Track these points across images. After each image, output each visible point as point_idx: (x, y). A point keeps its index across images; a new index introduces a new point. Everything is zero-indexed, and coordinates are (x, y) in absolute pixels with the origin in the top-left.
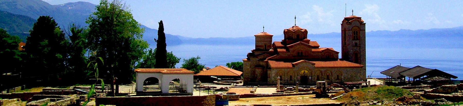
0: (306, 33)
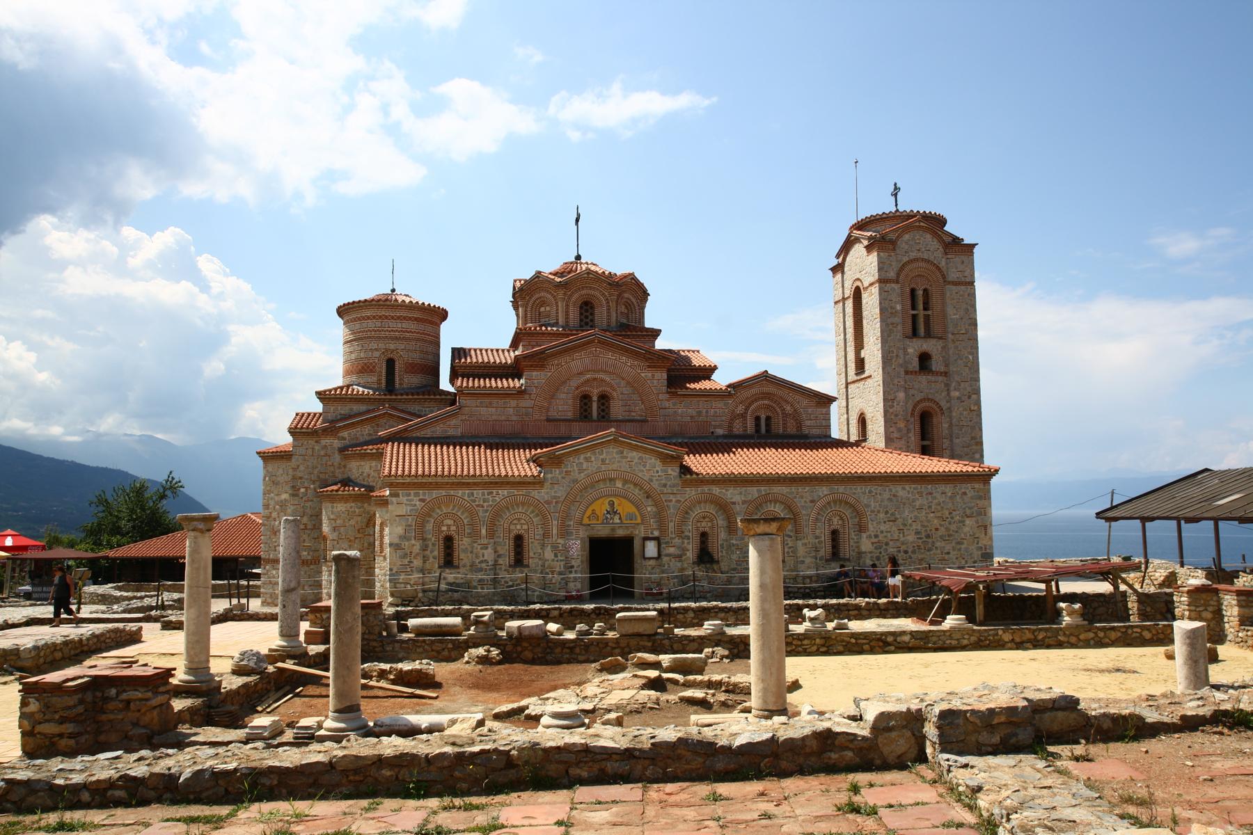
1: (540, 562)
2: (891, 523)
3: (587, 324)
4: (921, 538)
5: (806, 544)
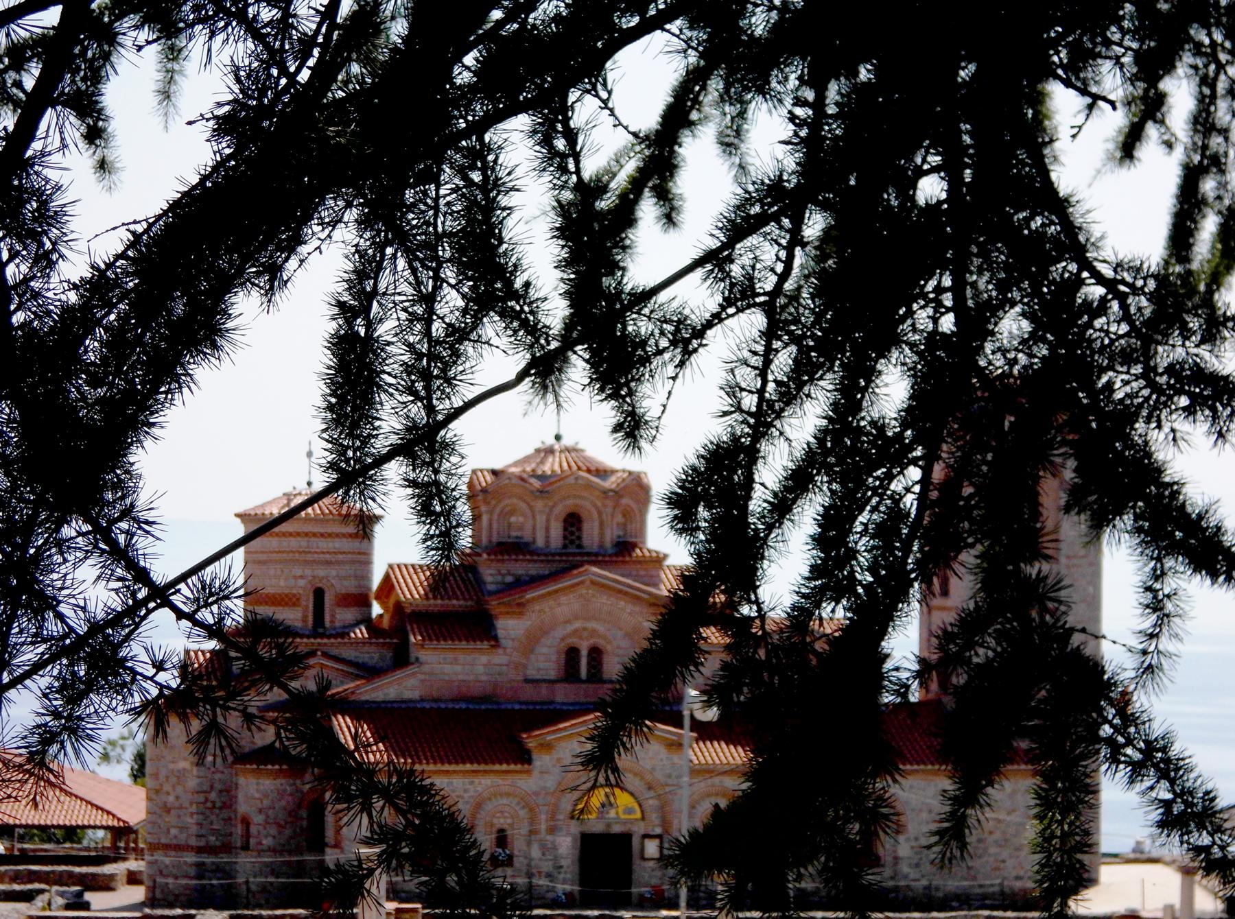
0: (638, 502)
3: (572, 542)
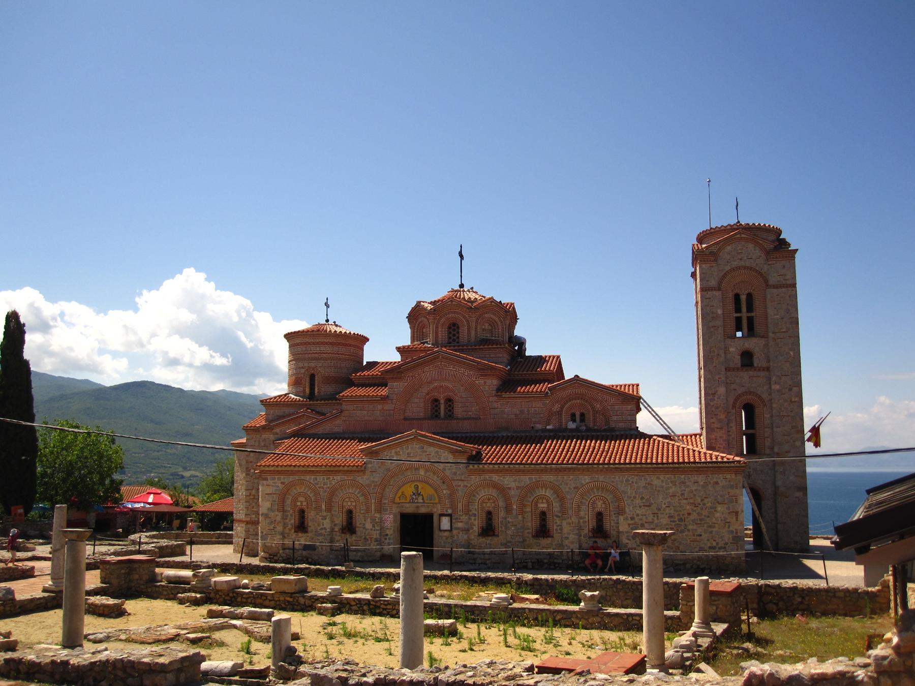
1: (364, 530)
2: (647, 508)
3: (454, 340)
4: (674, 521)
5: (570, 524)
